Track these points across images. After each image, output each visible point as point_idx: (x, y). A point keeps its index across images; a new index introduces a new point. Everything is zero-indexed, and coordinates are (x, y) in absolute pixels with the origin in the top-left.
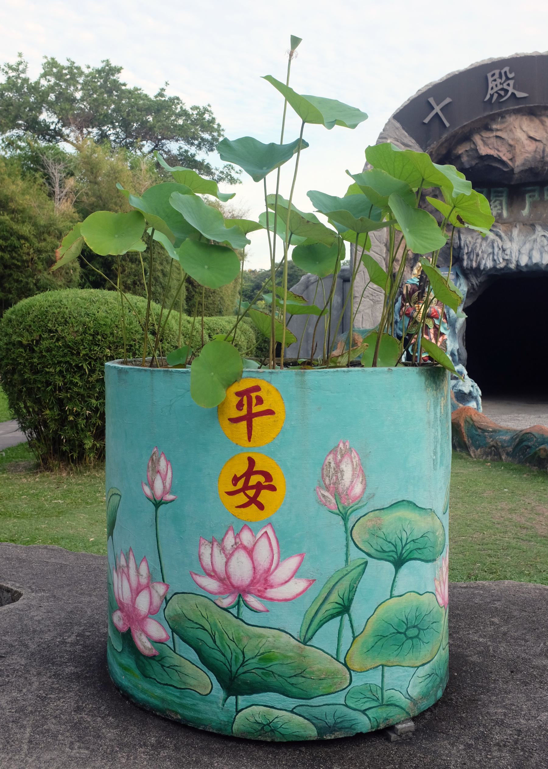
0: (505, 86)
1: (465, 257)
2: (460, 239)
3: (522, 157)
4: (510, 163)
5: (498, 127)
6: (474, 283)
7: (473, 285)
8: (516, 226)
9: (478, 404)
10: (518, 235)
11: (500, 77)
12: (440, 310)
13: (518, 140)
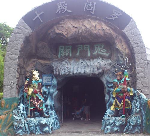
0: (64, 8)
1: (54, 70)
2: (53, 64)
3: (71, 34)
4: (66, 36)
5: (62, 23)
6: (59, 80)
7: (59, 81)
8: (73, 59)
9: (49, 129)
10: (74, 62)
11: (62, 5)
12: (38, 90)
13: (69, 28)
